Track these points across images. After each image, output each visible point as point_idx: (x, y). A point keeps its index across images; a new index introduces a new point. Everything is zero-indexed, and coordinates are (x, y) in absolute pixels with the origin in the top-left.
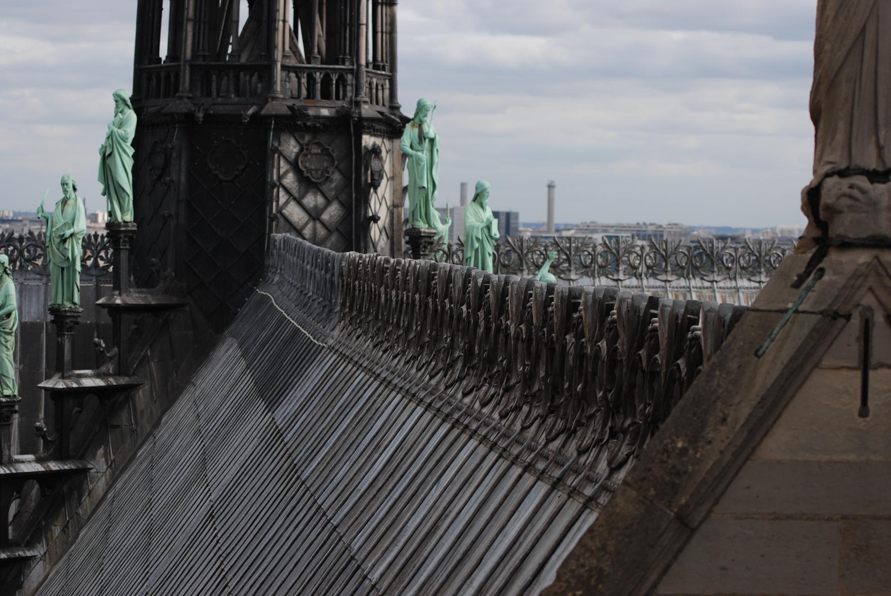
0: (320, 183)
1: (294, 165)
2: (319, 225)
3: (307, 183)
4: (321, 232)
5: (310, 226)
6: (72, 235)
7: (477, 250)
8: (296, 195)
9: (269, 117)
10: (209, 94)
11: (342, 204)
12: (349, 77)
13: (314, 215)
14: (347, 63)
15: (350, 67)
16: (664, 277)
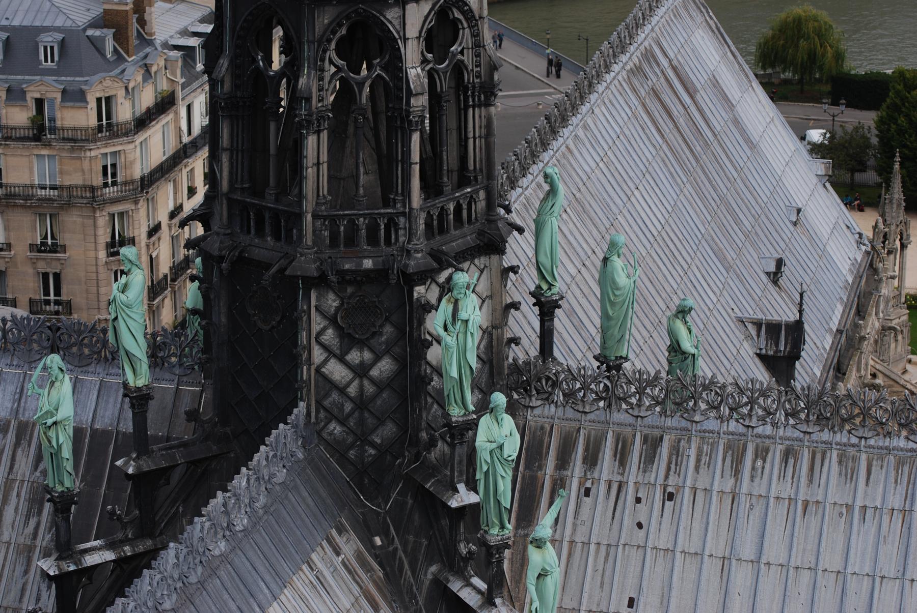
0: (367, 339)
1: (332, 321)
2: (366, 383)
3: (349, 340)
4: (370, 389)
5: (356, 383)
6: (55, 423)
7: (487, 473)
8: (338, 352)
9: (297, 277)
10: (249, 232)
11: (395, 359)
12: (402, 220)
13: (361, 371)
14: (399, 205)
15: (402, 209)
16: (804, 427)
